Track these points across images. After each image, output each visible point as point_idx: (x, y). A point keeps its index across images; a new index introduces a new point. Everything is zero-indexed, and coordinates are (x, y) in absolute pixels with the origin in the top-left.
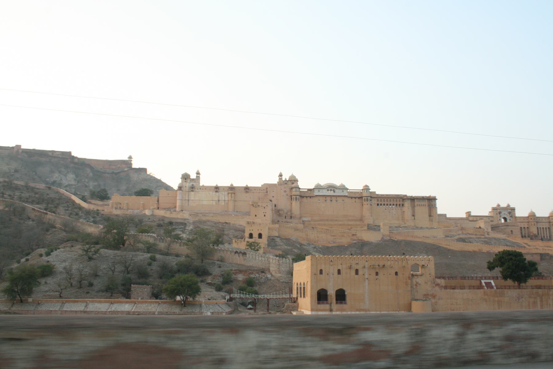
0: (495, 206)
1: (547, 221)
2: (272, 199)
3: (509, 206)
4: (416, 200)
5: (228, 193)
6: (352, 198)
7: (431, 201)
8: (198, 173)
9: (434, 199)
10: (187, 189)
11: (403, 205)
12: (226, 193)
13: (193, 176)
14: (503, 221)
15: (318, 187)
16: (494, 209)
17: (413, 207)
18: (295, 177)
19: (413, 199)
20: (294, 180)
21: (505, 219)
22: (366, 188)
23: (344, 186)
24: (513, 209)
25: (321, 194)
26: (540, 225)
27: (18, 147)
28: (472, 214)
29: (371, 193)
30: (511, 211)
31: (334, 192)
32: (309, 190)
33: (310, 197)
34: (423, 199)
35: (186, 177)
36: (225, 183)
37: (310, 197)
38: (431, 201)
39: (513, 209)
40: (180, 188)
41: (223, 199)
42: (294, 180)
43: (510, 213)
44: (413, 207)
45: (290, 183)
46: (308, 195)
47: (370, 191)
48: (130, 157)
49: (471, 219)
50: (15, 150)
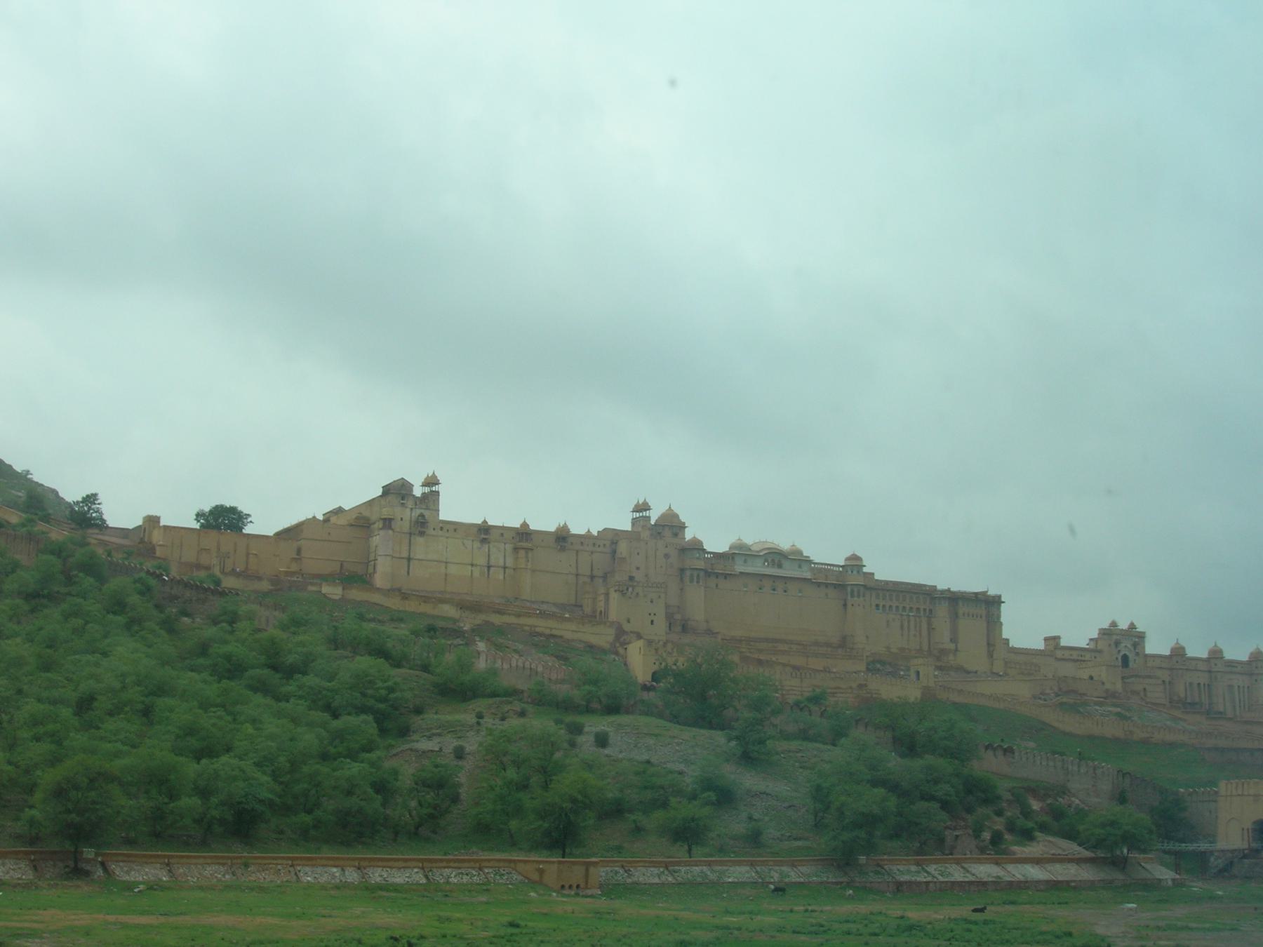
0: (1106, 625)
3: (1132, 626)
4: (960, 603)
5: (516, 549)
6: (819, 584)
7: (988, 605)
8: (431, 482)
9: (996, 602)
10: (406, 526)
11: (931, 611)
12: (509, 547)
13: (418, 491)
16: (1104, 633)
17: (955, 616)
18: (677, 516)
19: (954, 599)
22: (855, 563)
23: (800, 553)
24: (1142, 636)
25: (750, 569)
28: (1063, 643)
30: (1135, 637)
33: (726, 576)
36: (506, 516)
37: (726, 576)
38: (988, 605)
39: (1142, 636)
41: (501, 563)
43: (1135, 645)
44: (955, 616)
45: (667, 533)
47: (865, 570)
49: (1059, 654)
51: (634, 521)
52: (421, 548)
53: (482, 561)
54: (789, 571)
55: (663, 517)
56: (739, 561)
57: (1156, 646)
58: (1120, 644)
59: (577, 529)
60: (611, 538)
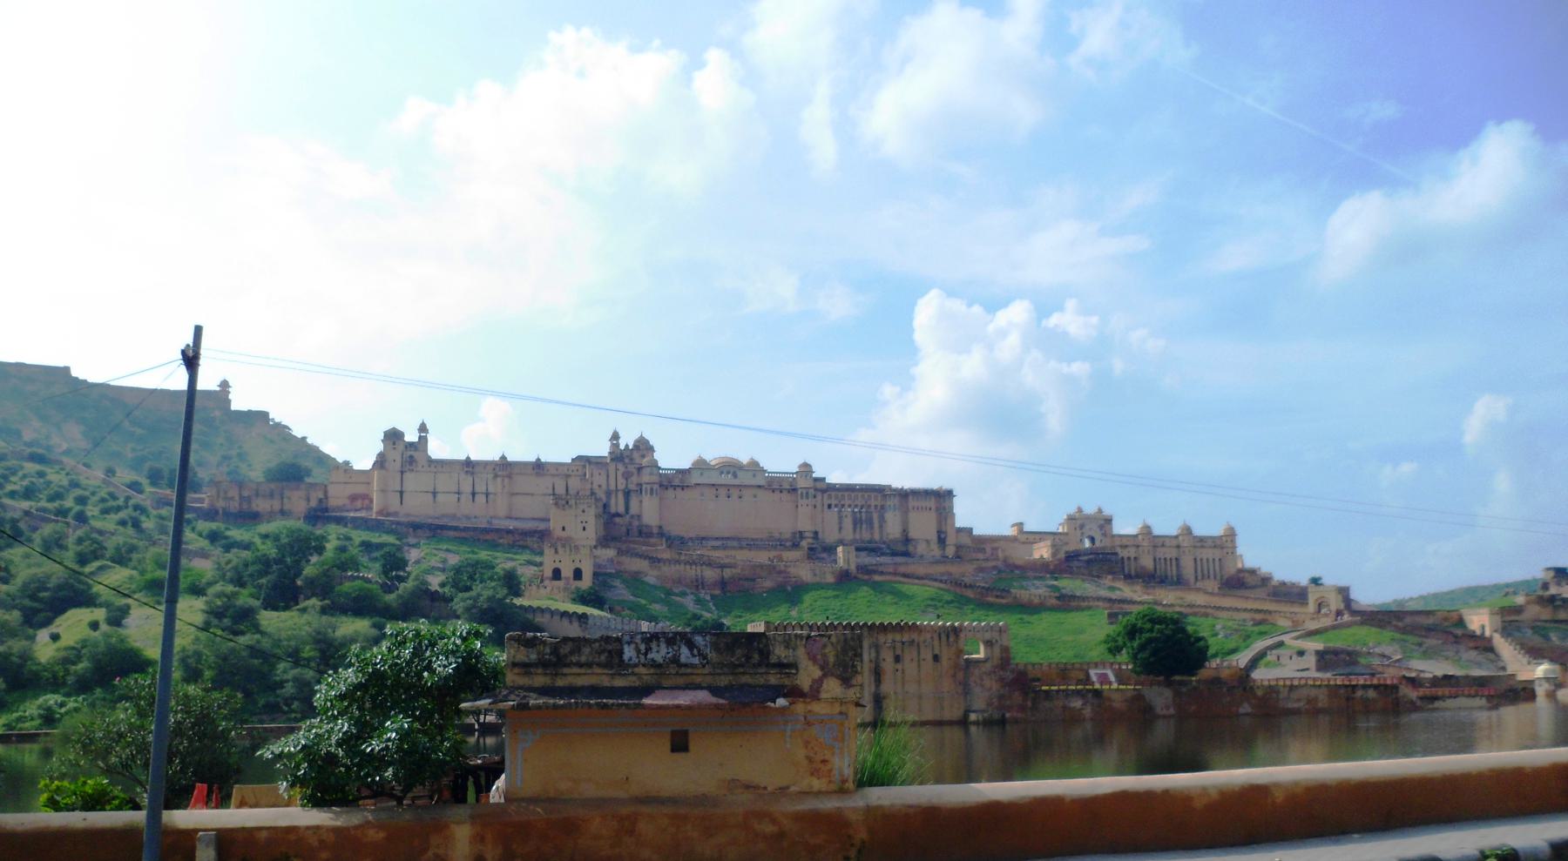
1: (1175, 543)
2: (597, 490)
5: (496, 476)
8: (423, 428)
10: (398, 465)
11: (883, 507)
13: (411, 436)
14: (1087, 544)
15: (701, 465)
16: (1071, 519)
19: (905, 495)
20: (643, 447)
21: (1092, 540)
22: (806, 468)
24: (1109, 521)
26: (1161, 553)
27: (66, 370)
28: (1026, 529)
29: (816, 480)
31: (735, 476)
32: (680, 471)
34: (927, 493)
35: (393, 436)
38: (941, 499)
40: (381, 462)
42: (643, 447)
43: (1101, 527)
44: (906, 512)
46: (676, 482)
48: (225, 385)
49: (1023, 538)
52: (411, 481)
53: (467, 488)
54: (744, 478)
57: (1125, 526)
60: (584, 461)
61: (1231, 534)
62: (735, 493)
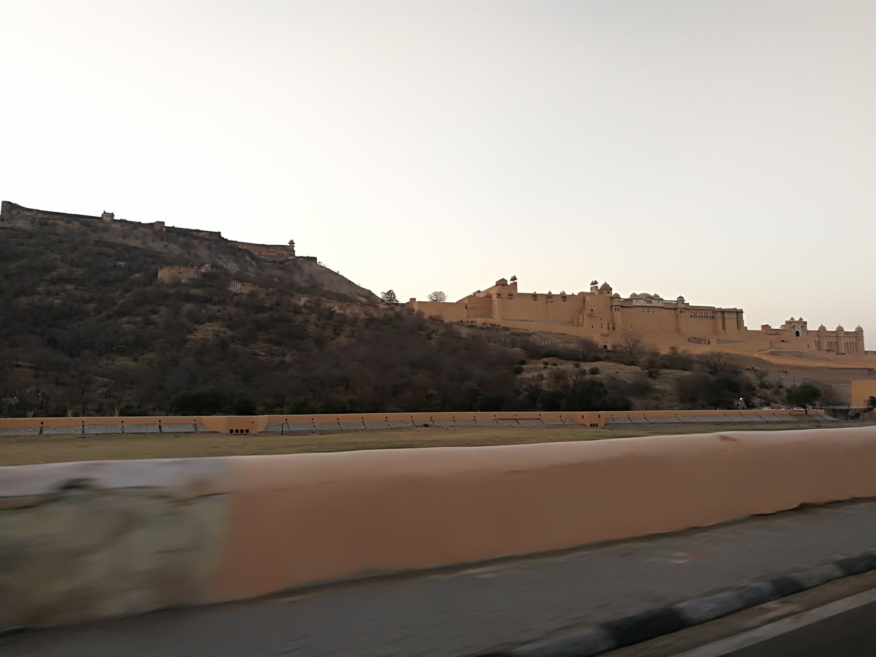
0: (788, 319)
1: (834, 335)
3: (801, 319)
7: (739, 313)
8: (514, 278)
9: (741, 312)
13: (509, 283)
15: (634, 297)
16: (787, 322)
19: (723, 312)
20: (607, 288)
24: (806, 323)
33: (630, 307)
37: (630, 307)
44: (724, 319)
48: (292, 243)
50: (157, 227)
51: (591, 288)
54: (654, 303)
55: (603, 286)
56: (634, 301)
57: (812, 327)
58: (796, 327)
59: (568, 293)
61: (860, 331)
62: (651, 309)
